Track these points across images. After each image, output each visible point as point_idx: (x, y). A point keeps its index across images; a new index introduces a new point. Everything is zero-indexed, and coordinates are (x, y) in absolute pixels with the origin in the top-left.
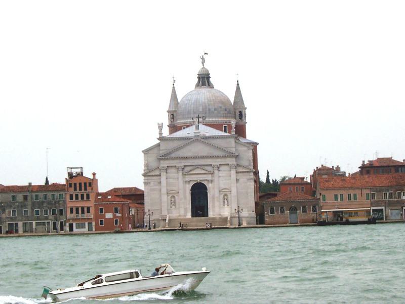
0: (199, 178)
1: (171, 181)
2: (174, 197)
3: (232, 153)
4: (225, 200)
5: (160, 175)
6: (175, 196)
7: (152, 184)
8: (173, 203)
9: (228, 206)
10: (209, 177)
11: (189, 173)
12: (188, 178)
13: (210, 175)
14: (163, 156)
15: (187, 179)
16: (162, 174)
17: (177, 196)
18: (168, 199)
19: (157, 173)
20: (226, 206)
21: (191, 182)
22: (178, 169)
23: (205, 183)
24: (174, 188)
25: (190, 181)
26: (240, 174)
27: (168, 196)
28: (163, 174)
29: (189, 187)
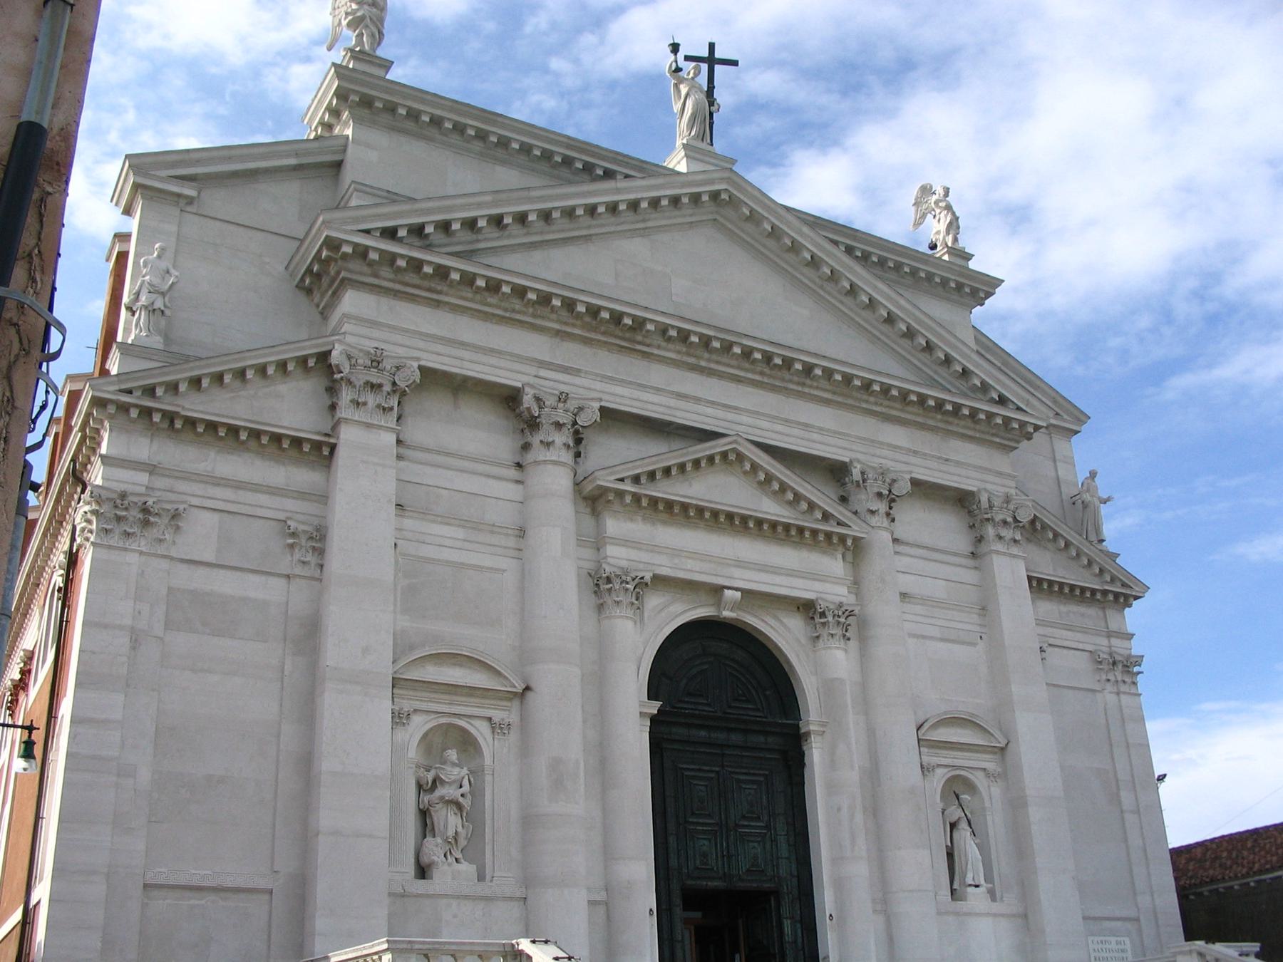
0: (745, 571)
1: (443, 541)
2: (467, 743)
3: (1002, 401)
4: (964, 833)
5: (322, 452)
6: (480, 731)
7: (201, 533)
8: (449, 822)
9: (992, 894)
10: (823, 578)
11: (665, 490)
12: (636, 543)
13: (835, 565)
14: (390, 233)
15: (617, 557)
16: (348, 436)
17: (498, 728)
18: (397, 751)
19: (291, 407)
20: (976, 899)
21: (653, 601)
22: (533, 424)
23: (786, 635)
24: (470, 638)
25: (660, 581)
26: (1050, 608)
27: (399, 719)
28: (364, 442)
29: (638, 639)
